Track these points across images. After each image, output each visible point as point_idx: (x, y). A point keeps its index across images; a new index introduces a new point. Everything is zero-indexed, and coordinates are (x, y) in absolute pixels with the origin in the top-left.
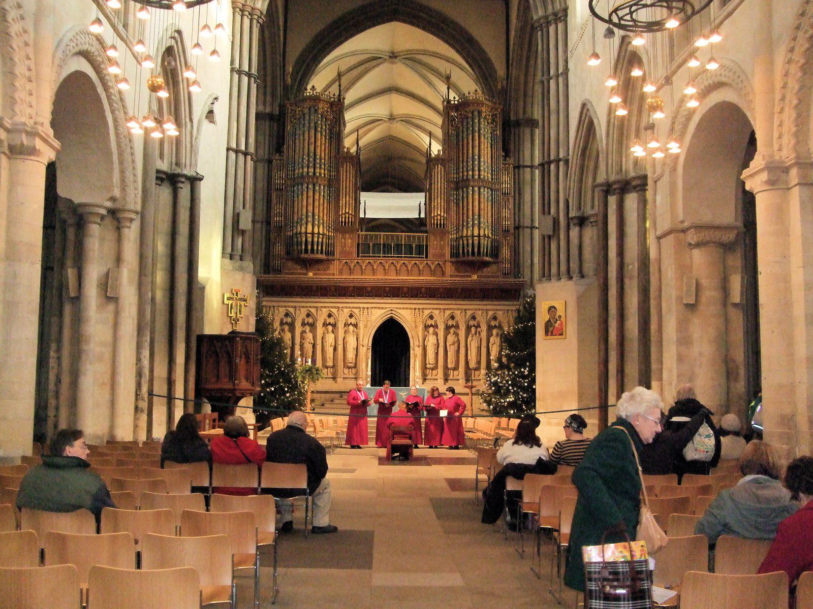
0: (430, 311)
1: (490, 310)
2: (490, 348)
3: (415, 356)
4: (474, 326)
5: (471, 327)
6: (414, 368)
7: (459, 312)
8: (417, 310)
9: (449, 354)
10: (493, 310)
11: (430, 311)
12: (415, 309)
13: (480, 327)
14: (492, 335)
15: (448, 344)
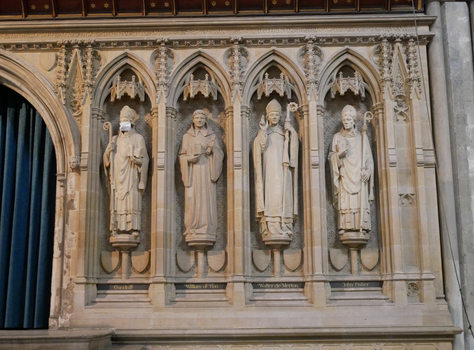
0: (118, 53)
1: (329, 41)
2: (335, 168)
3: (68, 205)
4: (274, 95)
5: (266, 100)
6: (62, 246)
7: (223, 51)
8: (76, 51)
9: (189, 193)
10: (341, 40)
11: (118, 53)
12: (69, 46)
13: (294, 98)
14: (340, 127)
15: (184, 160)
